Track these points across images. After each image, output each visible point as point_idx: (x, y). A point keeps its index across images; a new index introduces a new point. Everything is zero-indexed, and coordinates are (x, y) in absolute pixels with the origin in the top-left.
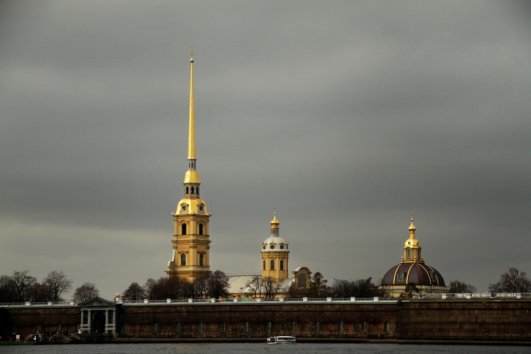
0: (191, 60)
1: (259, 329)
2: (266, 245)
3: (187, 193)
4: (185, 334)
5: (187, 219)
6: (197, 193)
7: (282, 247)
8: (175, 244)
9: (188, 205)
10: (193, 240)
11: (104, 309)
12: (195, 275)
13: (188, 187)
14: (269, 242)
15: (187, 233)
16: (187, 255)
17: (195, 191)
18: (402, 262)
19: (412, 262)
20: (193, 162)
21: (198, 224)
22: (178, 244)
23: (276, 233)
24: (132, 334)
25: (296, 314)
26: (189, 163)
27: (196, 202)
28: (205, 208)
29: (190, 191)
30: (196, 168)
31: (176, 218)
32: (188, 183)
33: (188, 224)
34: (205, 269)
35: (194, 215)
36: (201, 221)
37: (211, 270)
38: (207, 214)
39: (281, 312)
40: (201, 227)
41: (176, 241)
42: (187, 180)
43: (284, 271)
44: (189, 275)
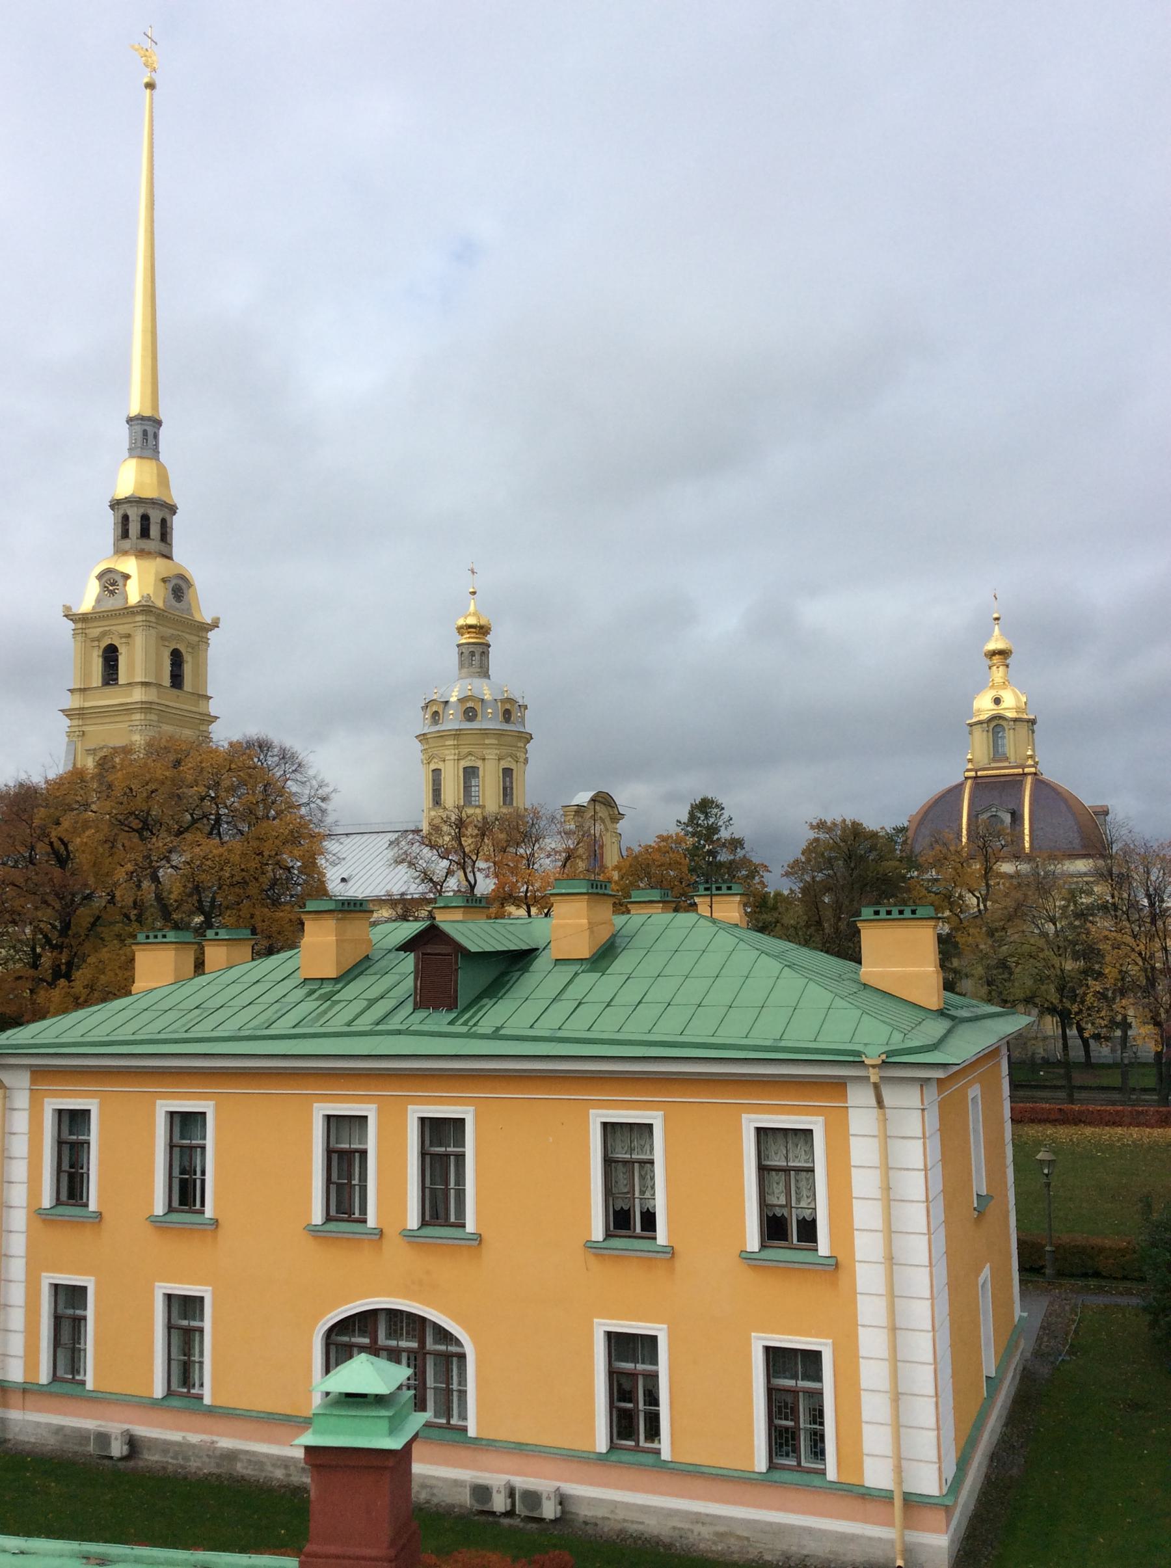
2: (444, 709)
3: (125, 534)
7: (507, 715)
9: (127, 577)
10: (142, 702)
14: (454, 694)
15: (121, 681)
17: (155, 531)
18: (972, 774)
19: (1020, 771)
22: (88, 722)
27: (156, 566)
29: (134, 528)
30: (159, 452)
36: (178, 638)
40: (177, 659)
41: (80, 709)
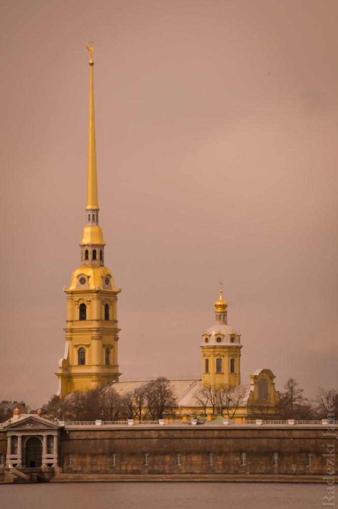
0: (91, 62)
1: (261, 463)
3: (87, 258)
4: (156, 468)
5: (86, 298)
6: (101, 258)
7: (232, 340)
8: (69, 334)
9: (89, 277)
10: (96, 328)
11: (40, 434)
12: (100, 379)
13: (88, 249)
15: (88, 317)
16: (87, 350)
17: (98, 256)
20: (95, 214)
21: (103, 304)
23: (224, 319)
24: (79, 469)
25: (313, 442)
26: (89, 215)
27: (100, 272)
28: (112, 281)
29: (90, 256)
31: (70, 295)
32: (88, 245)
33: (89, 304)
34: (113, 371)
35: (97, 292)
37: (120, 372)
38: (115, 290)
39: (292, 440)
41: (71, 329)
42: (87, 240)
43: (236, 374)
44: (91, 379)
